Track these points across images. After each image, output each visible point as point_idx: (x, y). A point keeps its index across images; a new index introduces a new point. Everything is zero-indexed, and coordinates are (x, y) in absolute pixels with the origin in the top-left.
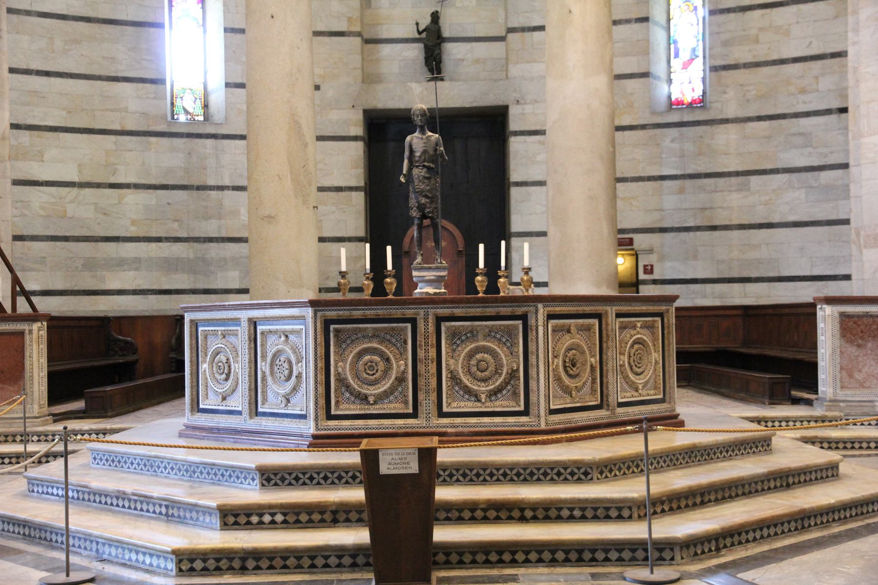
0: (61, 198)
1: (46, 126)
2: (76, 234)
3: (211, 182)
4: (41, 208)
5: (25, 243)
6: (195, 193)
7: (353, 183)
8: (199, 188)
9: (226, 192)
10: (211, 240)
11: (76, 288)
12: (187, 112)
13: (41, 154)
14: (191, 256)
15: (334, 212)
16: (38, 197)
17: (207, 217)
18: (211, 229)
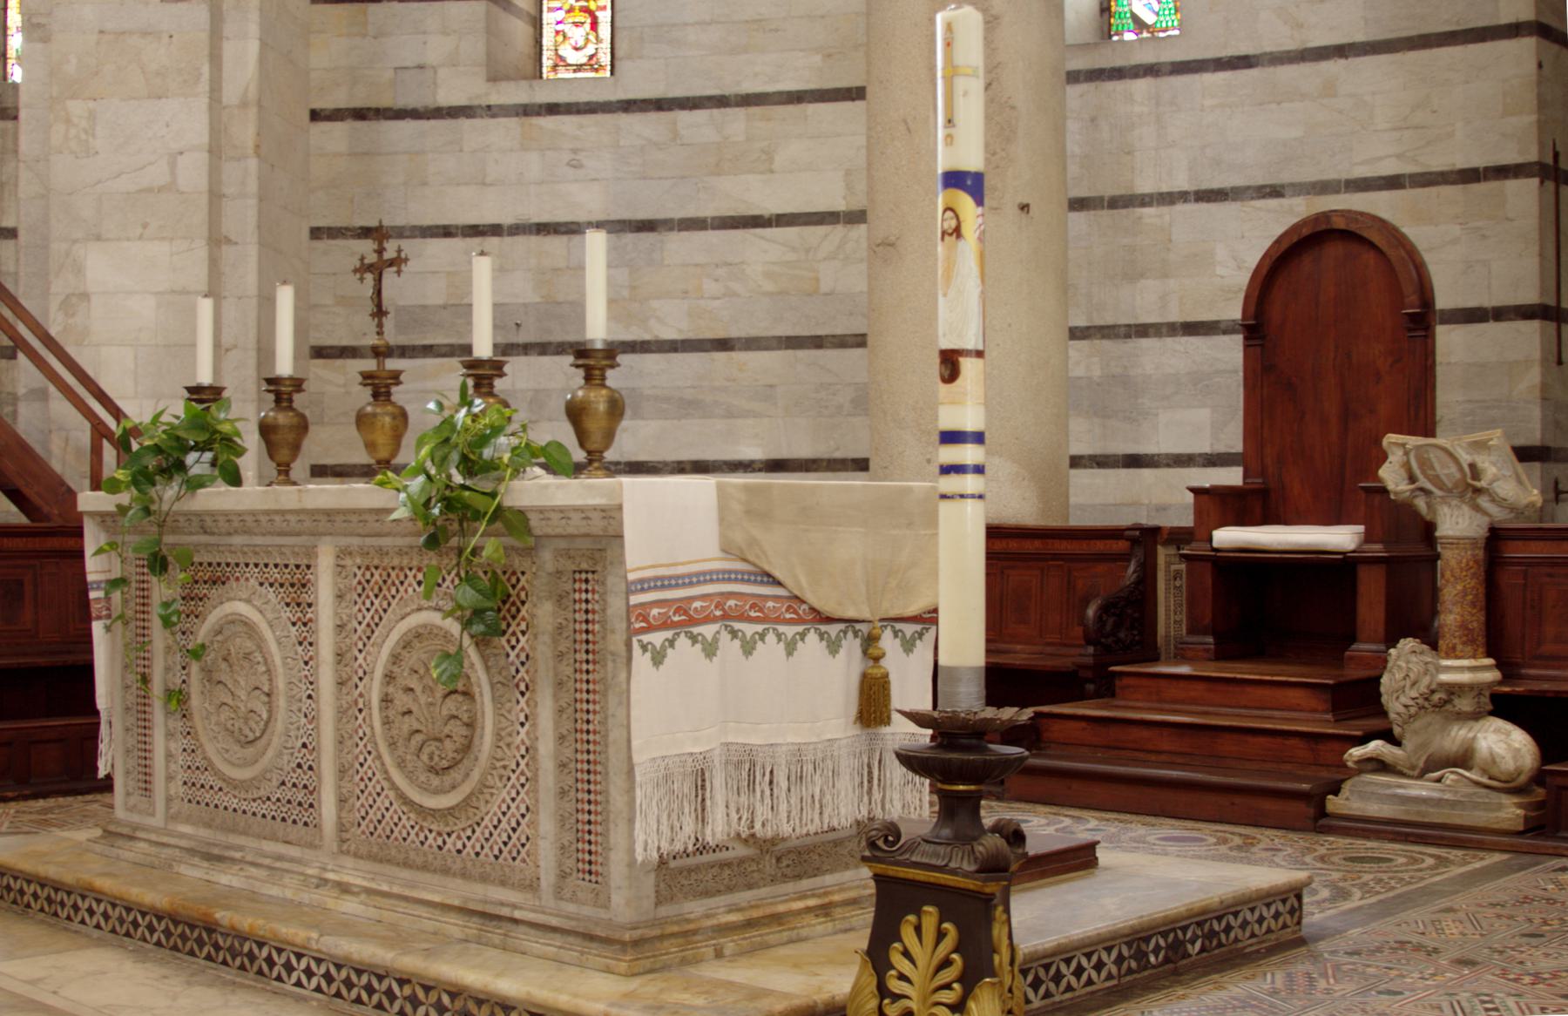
0: (807, 251)
1: (781, 93)
2: (839, 331)
3: (1145, 186)
4: (768, 275)
5: (733, 354)
6: (1105, 215)
7: (1510, 157)
8: (1115, 203)
9: (1180, 208)
10: (1143, 331)
11: (838, 455)
12: (1139, 24)
13: (769, 155)
14: (1097, 373)
15: (1455, 241)
16: (760, 252)
17: (1133, 274)
18: (1145, 304)
